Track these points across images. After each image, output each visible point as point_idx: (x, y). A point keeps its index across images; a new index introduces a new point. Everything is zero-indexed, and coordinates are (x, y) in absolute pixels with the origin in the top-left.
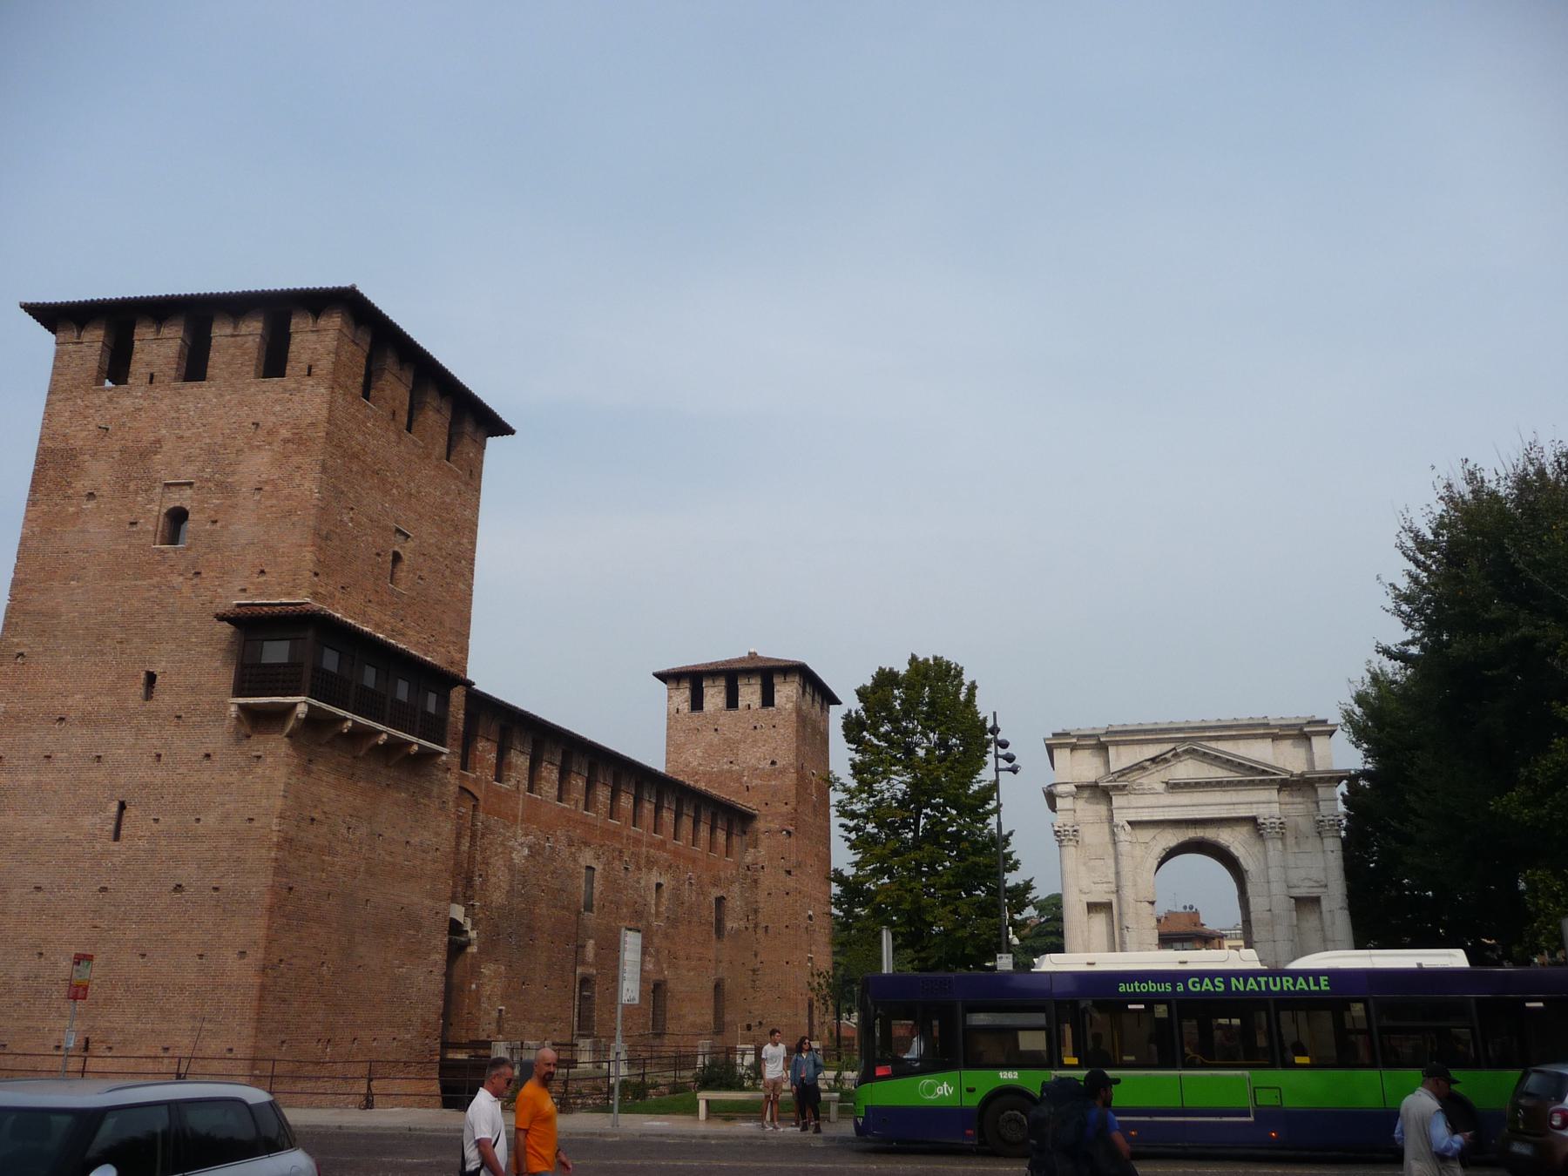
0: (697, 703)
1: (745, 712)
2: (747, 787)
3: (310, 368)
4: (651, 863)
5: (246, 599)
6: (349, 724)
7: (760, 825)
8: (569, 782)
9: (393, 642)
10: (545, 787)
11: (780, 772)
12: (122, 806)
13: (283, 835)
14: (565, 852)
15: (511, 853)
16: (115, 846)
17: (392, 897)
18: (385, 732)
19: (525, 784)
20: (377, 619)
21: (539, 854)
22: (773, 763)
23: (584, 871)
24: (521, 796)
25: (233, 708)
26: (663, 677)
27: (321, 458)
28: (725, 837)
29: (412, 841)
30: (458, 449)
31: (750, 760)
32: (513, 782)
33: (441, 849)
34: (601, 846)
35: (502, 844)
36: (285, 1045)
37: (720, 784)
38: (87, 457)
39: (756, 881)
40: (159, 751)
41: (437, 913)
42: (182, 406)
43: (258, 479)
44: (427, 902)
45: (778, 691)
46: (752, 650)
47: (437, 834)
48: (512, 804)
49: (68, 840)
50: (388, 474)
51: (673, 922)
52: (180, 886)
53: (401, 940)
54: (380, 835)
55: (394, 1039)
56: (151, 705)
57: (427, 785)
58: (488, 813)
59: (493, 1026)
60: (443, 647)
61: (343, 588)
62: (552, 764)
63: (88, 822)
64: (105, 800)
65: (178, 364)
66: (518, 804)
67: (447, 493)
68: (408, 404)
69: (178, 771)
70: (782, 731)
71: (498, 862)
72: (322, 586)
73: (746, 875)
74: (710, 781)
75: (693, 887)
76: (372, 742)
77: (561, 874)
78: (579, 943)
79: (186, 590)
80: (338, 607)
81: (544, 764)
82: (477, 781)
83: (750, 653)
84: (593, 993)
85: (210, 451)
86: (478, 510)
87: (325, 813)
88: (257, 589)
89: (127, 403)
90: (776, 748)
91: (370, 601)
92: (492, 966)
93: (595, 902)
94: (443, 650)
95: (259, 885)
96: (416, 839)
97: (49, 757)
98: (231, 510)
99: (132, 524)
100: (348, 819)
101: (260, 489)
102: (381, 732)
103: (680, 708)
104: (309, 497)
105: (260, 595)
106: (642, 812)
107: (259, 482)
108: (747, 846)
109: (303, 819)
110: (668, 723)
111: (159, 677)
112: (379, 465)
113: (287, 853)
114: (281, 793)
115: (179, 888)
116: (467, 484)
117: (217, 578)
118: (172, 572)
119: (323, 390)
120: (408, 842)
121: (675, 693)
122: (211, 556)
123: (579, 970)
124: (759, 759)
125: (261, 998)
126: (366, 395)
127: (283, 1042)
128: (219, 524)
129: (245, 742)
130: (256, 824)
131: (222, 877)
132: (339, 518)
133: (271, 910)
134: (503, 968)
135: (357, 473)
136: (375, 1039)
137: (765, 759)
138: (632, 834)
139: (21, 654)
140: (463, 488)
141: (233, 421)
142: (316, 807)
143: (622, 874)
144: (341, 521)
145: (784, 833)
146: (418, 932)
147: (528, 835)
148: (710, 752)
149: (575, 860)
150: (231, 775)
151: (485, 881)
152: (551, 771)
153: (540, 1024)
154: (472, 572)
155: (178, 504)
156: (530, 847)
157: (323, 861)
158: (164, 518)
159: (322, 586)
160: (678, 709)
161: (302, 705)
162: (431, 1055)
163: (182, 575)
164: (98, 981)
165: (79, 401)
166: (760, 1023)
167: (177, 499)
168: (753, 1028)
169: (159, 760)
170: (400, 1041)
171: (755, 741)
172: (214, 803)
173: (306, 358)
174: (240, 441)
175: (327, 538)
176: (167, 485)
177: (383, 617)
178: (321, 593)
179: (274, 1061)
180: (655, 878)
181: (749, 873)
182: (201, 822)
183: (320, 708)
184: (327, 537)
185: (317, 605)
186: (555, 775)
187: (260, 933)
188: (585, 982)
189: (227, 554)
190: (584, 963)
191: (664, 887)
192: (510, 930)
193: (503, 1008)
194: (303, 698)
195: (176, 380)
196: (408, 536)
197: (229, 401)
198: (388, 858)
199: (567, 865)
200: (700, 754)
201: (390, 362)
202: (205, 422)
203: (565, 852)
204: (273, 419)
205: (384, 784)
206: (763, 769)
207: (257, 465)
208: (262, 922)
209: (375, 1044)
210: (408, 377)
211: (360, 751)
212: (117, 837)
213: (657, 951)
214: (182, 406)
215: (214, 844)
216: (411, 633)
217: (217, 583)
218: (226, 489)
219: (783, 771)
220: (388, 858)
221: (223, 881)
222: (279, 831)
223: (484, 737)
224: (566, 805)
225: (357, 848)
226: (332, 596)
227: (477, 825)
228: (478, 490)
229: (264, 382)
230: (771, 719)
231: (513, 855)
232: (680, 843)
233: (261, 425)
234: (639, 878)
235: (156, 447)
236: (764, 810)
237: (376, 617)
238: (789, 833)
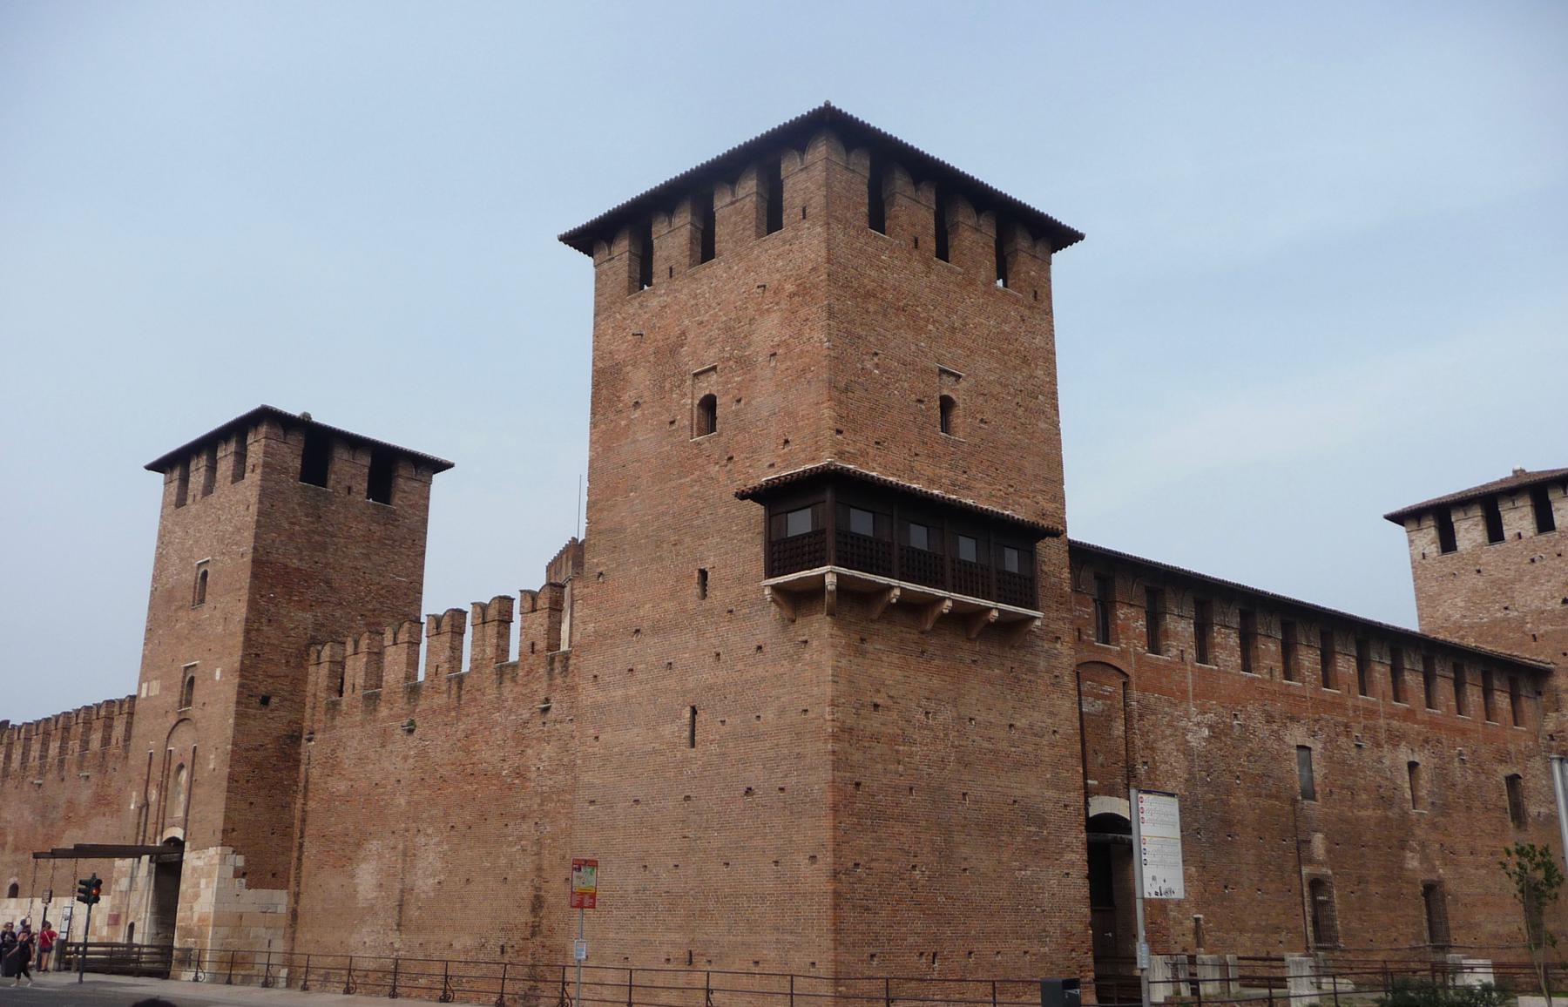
0: (1447, 542)
1: (1515, 543)
2: (1534, 636)
3: (804, 211)
4: (1395, 739)
5: (775, 474)
6: (897, 592)
9: (954, 497)
10: (1221, 655)
12: (694, 711)
13: (839, 724)
14: (1264, 731)
15: (1184, 735)
16: (692, 753)
18: (949, 598)
19: (1191, 654)
20: (931, 475)
21: (1226, 735)
23: (1295, 751)
24: (1189, 668)
25: (767, 592)
26: (1398, 518)
27: (826, 303)
28: (1508, 700)
29: (1018, 724)
30: (1014, 270)
31: (1532, 601)
32: (1174, 652)
33: (1061, 731)
34: (1316, 721)
35: (1170, 725)
36: (875, 959)
37: (1495, 636)
38: (629, 368)
40: (717, 650)
41: (1066, 806)
42: (698, 291)
43: (772, 344)
44: (1050, 793)
46: (1517, 467)
47: (1052, 714)
48: (1177, 678)
49: (655, 751)
50: (918, 309)
51: (1444, 809)
52: (750, 789)
53: (1019, 839)
54: (971, 719)
55: (1025, 953)
56: (706, 604)
57: (1029, 658)
58: (1145, 690)
59: (1190, 938)
60: (1029, 498)
61: (877, 443)
62: (1227, 627)
63: (668, 730)
64: (680, 707)
65: (691, 250)
66: (1185, 677)
67: (1005, 321)
68: (933, 227)
69: (736, 668)
71: (1167, 748)
72: (848, 444)
74: (1481, 635)
75: (1468, 765)
76: (936, 612)
77: (1261, 756)
79: (722, 478)
80: (875, 466)
81: (1216, 629)
82: (1123, 654)
83: (1515, 472)
84: (1331, 897)
85: (727, 329)
86: (1053, 336)
87: (892, 697)
88: (783, 461)
89: (654, 303)
91: (916, 455)
93: (1317, 789)
94: (1029, 501)
95: (819, 781)
96: (1023, 721)
97: (631, 670)
98: (752, 384)
99: (672, 423)
100: (924, 702)
101: (774, 354)
102: (943, 599)
103: (1425, 552)
104: (820, 349)
105: (787, 467)
106: (1371, 676)
107: (772, 347)
108: (1546, 710)
109: (862, 705)
110: (1414, 573)
111: (709, 574)
112: (905, 301)
113: (847, 745)
114: (830, 678)
115: (749, 791)
116: (1031, 307)
117: (747, 458)
118: (709, 463)
119: (819, 230)
120: (1011, 726)
121: (1416, 536)
122: (740, 437)
123: (1305, 870)
124: (1545, 599)
125: (836, 907)
126: (943, 253)
127: (873, 956)
128: (742, 402)
129: (791, 628)
130: (810, 715)
131: (786, 776)
132: (859, 366)
133: (835, 809)
134: (1194, 869)
135: (876, 313)
136: (998, 953)
138: (1360, 703)
139: (601, 574)
140: (1027, 313)
141: (743, 290)
142: (878, 691)
143: (1354, 752)
144: (863, 369)
146: (1040, 827)
147: (1206, 713)
148: (1474, 599)
149: (1280, 739)
150: (782, 666)
151: (1153, 769)
152: (1228, 636)
153: (1256, 935)
154: (1056, 408)
155: (707, 392)
156: (1210, 727)
157: (897, 752)
158: (698, 410)
159: (848, 444)
160: (1424, 554)
161: (829, 574)
162: (1081, 972)
163: (717, 463)
164: (692, 892)
165: (618, 316)
167: (708, 386)
169: (719, 659)
170: (1034, 955)
171: (1535, 579)
172: (770, 697)
173: (798, 201)
174: (751, 312)
175: (846, 390)
176: (696, 375)
177: (937, 471)
178: (848, 452)
179: (792, 976)
180: (1404, 755)
181: (1553, 743)
182: (762, 719)
183: (853, 577)
184: (846, 389)
185: (840, 464)
186: (1234, 640)
187: (827, 835)
188: (1316, 884)
189: (753, 431)
190: (1310, 861)
191: (1421, 767)
192: (1196, 825)
193: (1201, 916)
194: (828, 568)
195: (691, 266)
196: (959, 376)
197: (737, 271)
198: (986, 745)
199: (1268, 746)
200: (1462, 604)
201: (900, 183)
202: (719, 300)
204: (778, 276)
205: (968, 661)
206: (1553, 611)
207: (769, 329)
208: (827, 823)
209: (999, 958)
210: (929, 197)
211: (926, 624)
212: (693, 745)
213: (1423, 845)
214: (698, 291)
215: (775, 741)
216: (978, 486)
217: (748, 464)
218: (745, 363)
220: (986, 745)
221: (788, 780)
222: (833, 720)
223: (1125, 603)
224: (1257, 675)
225: (942, 735)
226: (864, 454)
227: (1131, 705)
228: (1049, 312)
229: (764, 241)
230: (1554, 546)
231: (1188, 738)
232: (1439, 712)
233: (767, 286)
234: (1380, 757)
235: (682, 340)
237: (929, 472)
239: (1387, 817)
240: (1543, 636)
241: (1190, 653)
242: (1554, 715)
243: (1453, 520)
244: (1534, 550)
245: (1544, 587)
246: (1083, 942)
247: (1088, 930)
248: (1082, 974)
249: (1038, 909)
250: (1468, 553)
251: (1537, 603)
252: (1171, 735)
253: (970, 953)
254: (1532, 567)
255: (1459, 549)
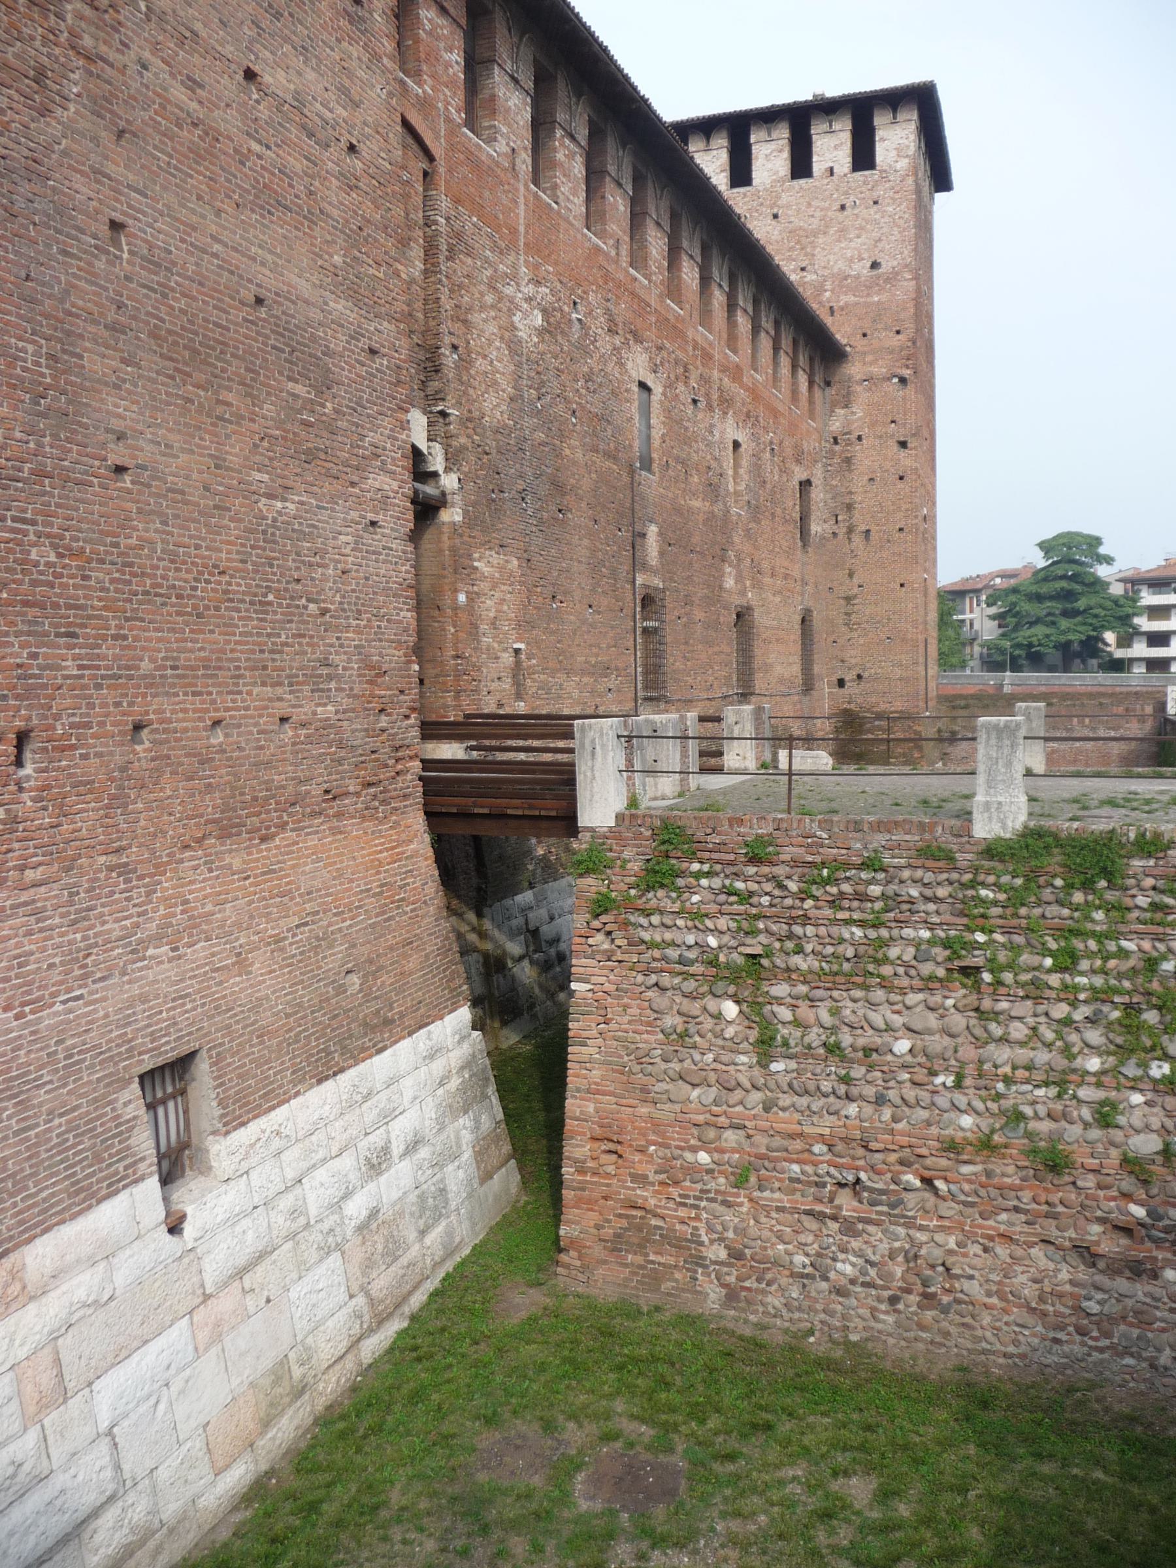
7: (854, 369)
8: (603, 197)
11: (887, 281)
17: (217, 247)
22: (875, 265)
32: (502, 146)
34: (660, 348)
39: (848, 461)
41: (373, 352)
44: (340, 307)
45: (883, 140)
53: (268, 409)
55: (283, 720)
59: (507, 684)
70: (890, 209)
71: (486, 326)
73: (833, 453)
77: (600, 385)
78: (638, 528)
90: (880, 240)
92: (496, 558)
93: (655, 455)
108: (834, 405)
124: (851, 260)
134: (516, 562)
136: (217, 723)
137: (861, 259)
145: (896, 380)
146: (320, 393)
151: (465, 363)
153: (585, 680)
162: (397, 760)
166: (859, 677)
168: (848, 684)
171: (843, 230)
181: (837, 448)
188: (648, 601)
198: (178, 93)
203: (605, 344)
206: (858, 277)
209: (218, 738)
219: (893, 278)
227: (436, 223)
231: (516, 319)
236: (860, 343)
238: (903, 380)
239: (712, 512)
240: (842, 309)
241: (524, 162)
242: (842, 412)
243: (752, 140)
244: (846, 193)
245: (852, 245)
246: (402, 692)
247: (409, 662)
248: (399, 767)
249: (312, 607)
250: (766, 190)
251: (841, 265)
252: (493, 306)
253: (138, 727)
254: (840, 216)
255: (754, 182)
